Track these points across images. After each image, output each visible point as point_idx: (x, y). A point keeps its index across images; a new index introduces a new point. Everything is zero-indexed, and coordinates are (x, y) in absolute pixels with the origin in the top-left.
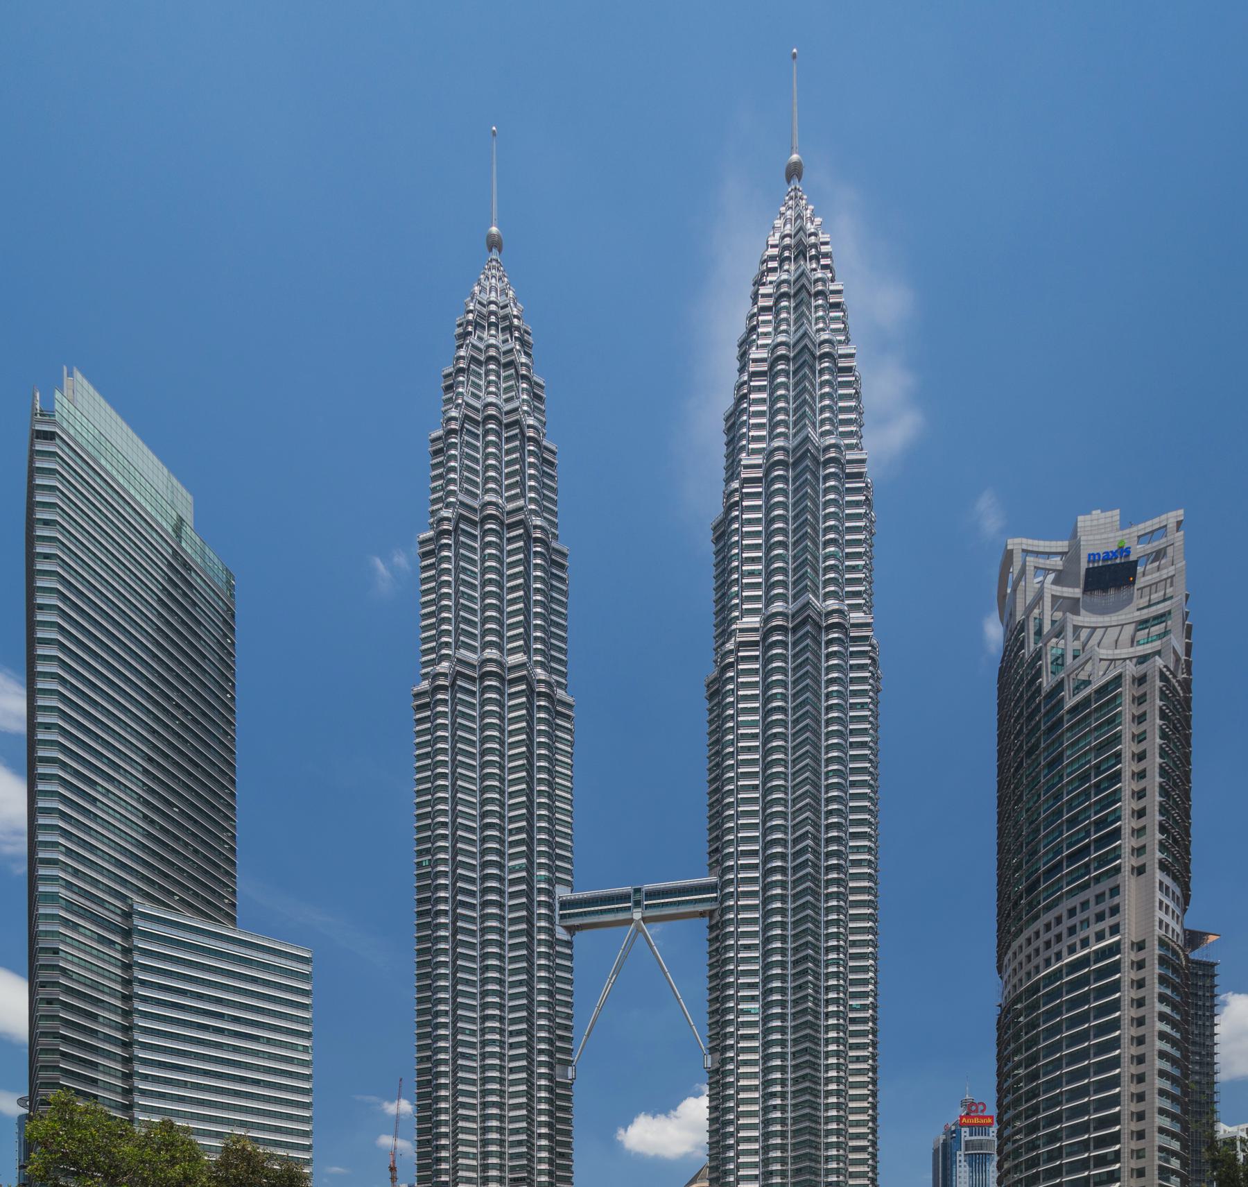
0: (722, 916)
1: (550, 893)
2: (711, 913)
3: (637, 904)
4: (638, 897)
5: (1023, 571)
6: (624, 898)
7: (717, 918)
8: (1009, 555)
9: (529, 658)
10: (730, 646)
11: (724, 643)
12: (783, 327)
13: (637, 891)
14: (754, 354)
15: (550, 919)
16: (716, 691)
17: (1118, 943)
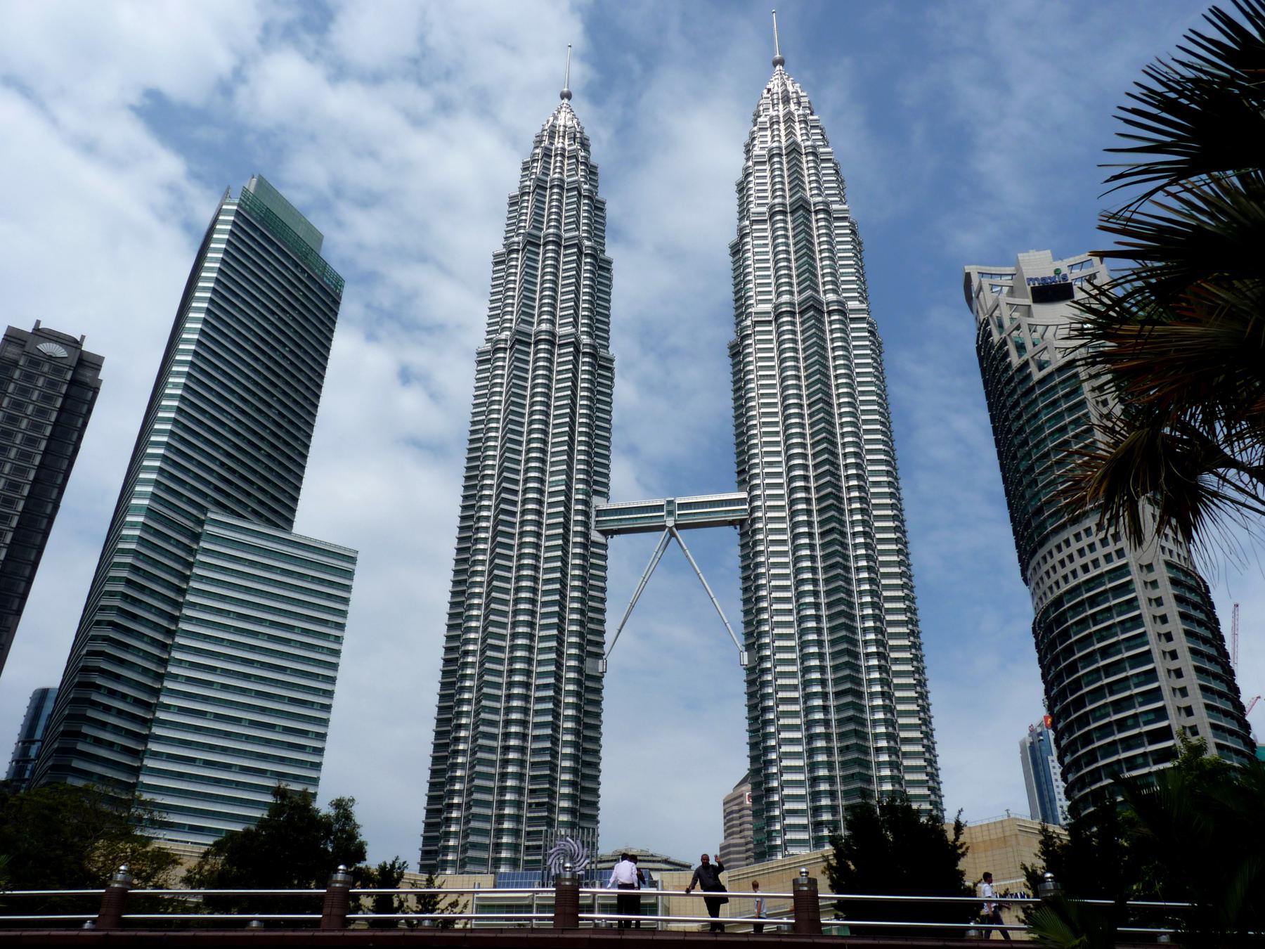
0: (751, 525)
1: (586, 503)
2: (742, 522)
3: (670, 513)
4: (670, 508)
5: (980, 289)
6: (660, 508)
7: (747, 527)
8: (968, 276)
9: (577, 330)
10: (748, 322)
11: (742, 321)
12: (776, 139)
13: (670, 503)
14: (757, 151)
15: (586, 524)
16: (737, 352)
17: (1126, 565)
